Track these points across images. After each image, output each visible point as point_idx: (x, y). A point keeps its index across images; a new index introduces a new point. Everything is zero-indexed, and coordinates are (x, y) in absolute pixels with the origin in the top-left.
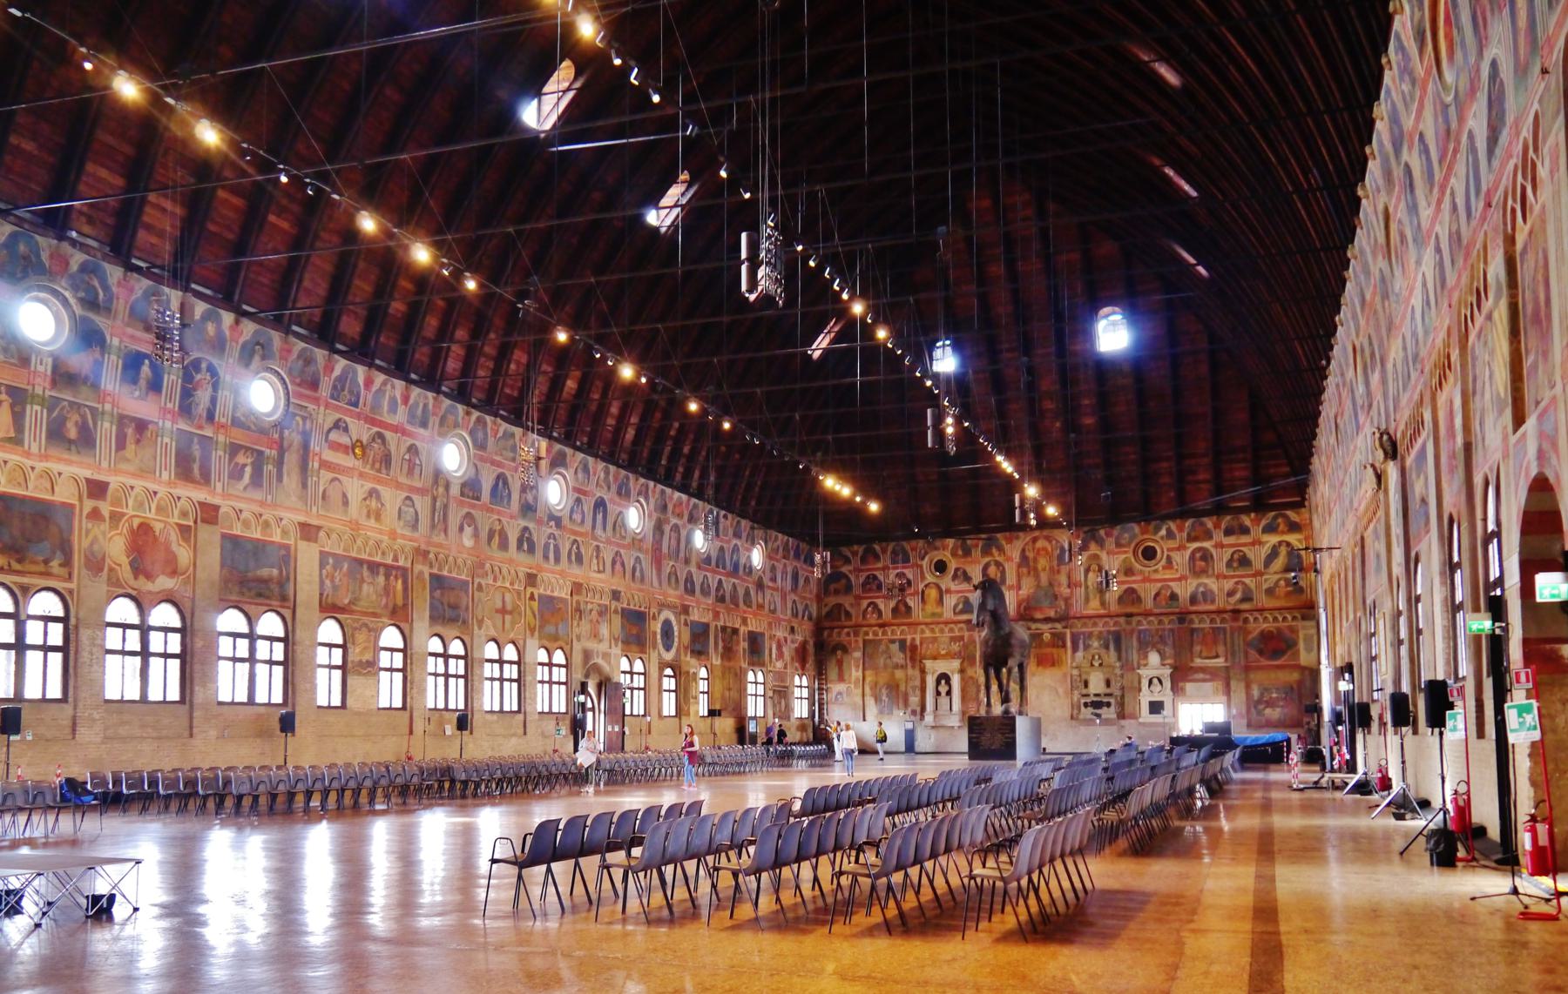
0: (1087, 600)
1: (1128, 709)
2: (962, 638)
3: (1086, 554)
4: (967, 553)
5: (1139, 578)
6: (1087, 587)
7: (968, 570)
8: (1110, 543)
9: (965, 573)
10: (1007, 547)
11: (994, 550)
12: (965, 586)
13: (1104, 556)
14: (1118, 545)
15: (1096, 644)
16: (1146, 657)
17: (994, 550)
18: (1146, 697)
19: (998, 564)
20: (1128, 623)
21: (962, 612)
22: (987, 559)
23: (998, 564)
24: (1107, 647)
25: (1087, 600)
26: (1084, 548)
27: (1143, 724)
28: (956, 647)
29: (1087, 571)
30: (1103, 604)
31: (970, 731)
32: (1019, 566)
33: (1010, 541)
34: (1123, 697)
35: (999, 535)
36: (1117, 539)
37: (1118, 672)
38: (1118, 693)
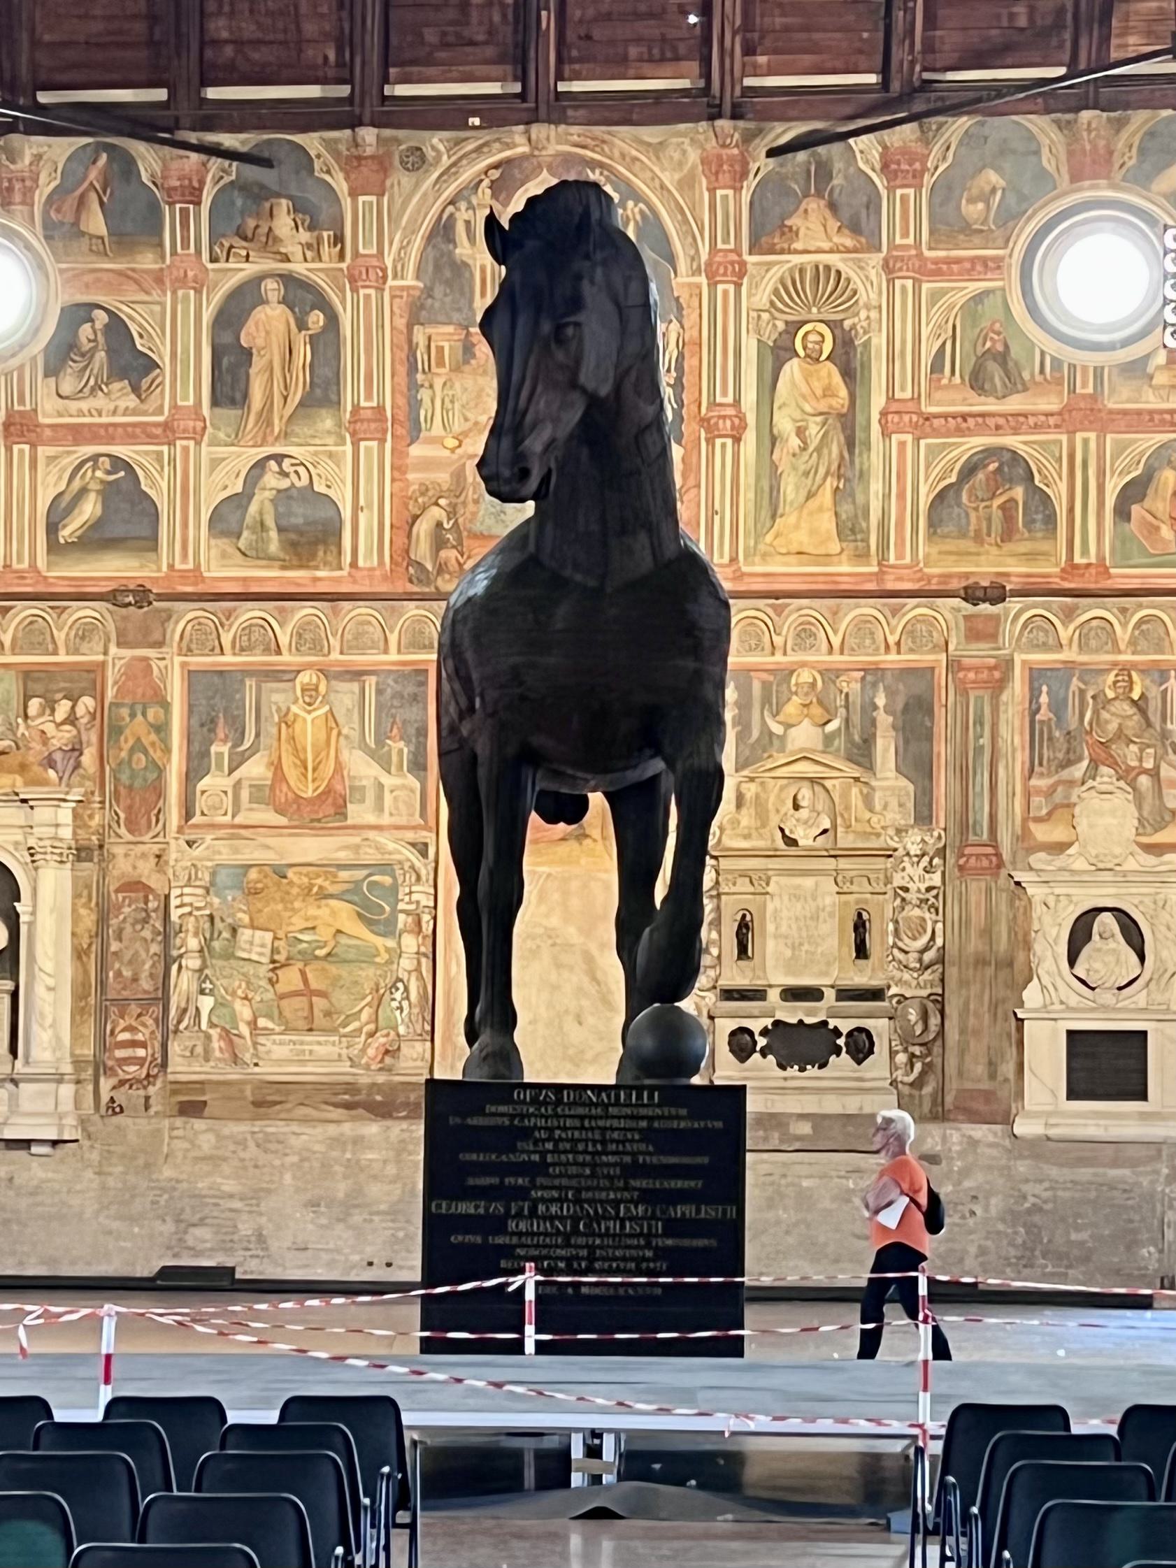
0: (771, 504)
1: (966, 1068)
2: (91, 680)
3: (767, 275)
4: (136, 223)
5: (1050, 403)
6: (772, 440)
7: (139, 319)
8: (904, 215)
9: (117, 328)
10: (356, 210)
11: (283, 223)
12: (116, 404)
13: (865, 278)
14: (949, 226)
15: (804, 735)
16: (1063, 809)
17: (283, 223)
18: (1054, 1009)
19: (301, 296)
20: (979, 632)
21: (97, 540)
22: (241, 270)
23: (301, 296)
24: (862, 753)
25: (771, 504)
26: (768, 231)
27: (1038, 1148)
28: (50, 727)
29: (779, 353)
30: (850, 529)
31: (442, 1176)
32: (417, 313)
33: (371, 174)
34: (940, 1002)
35: (311, 141)
36: (946, 193)
37: (914, 877)
38: (909, 985)
